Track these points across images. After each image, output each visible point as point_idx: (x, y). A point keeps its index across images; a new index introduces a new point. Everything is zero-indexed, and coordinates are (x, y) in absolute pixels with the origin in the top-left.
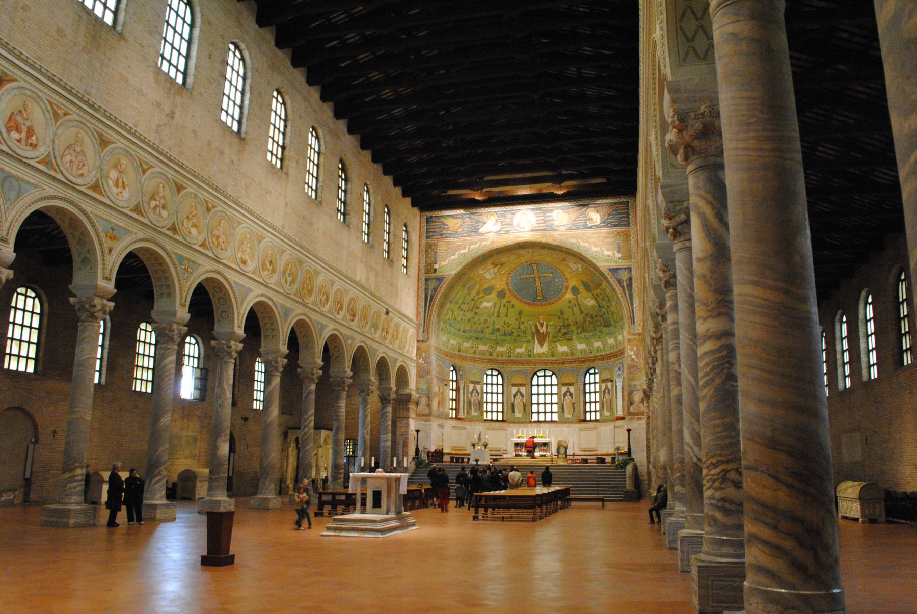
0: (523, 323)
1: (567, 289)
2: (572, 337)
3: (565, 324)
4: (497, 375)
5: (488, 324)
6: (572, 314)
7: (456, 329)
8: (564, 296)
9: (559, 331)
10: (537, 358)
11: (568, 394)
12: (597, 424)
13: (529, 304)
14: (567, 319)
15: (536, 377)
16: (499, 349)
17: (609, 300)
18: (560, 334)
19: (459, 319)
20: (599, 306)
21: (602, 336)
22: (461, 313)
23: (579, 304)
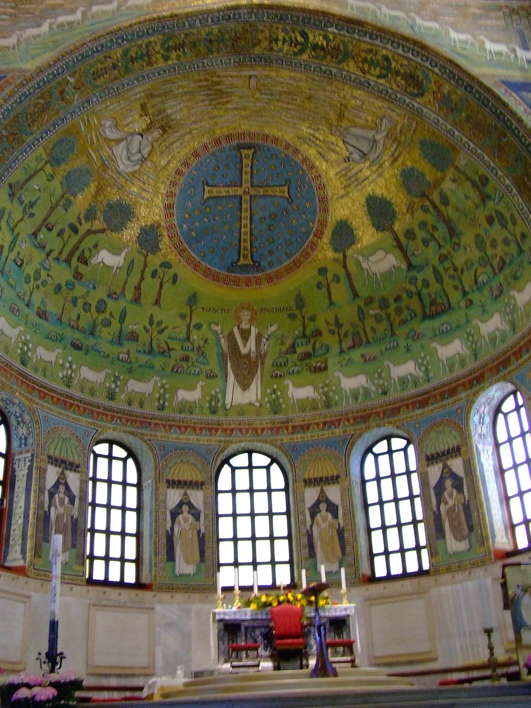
0: (198, 327)
1: (319, 235)
2: (326, 362)
3: (308, 333)
4: (124, 460)
5: (107, 315)
6: (327, 301)
7: (18, 295)
8: (306, 255)
9: (293, 349)
10: (233, 417)
11: (323, 506)
12: (424, 580)
13: (216, 278)
14: (313, 319)
15: (226, 470)
16: (134, 385)
17: (452, 232)
18: (293, 358)
19: (30, 269)
20: (410, 266)
21: (416, 346)
22: (39, 256)
23: (348, 275)
